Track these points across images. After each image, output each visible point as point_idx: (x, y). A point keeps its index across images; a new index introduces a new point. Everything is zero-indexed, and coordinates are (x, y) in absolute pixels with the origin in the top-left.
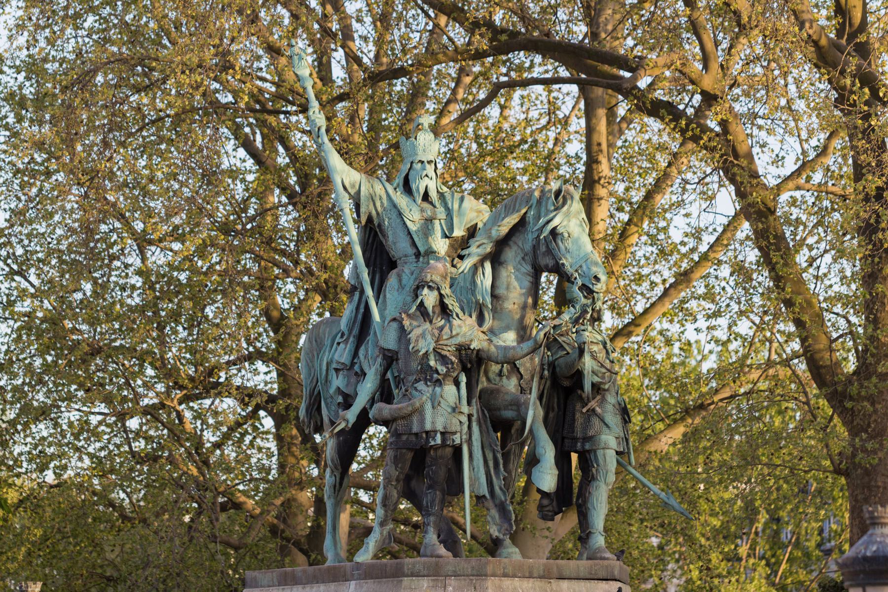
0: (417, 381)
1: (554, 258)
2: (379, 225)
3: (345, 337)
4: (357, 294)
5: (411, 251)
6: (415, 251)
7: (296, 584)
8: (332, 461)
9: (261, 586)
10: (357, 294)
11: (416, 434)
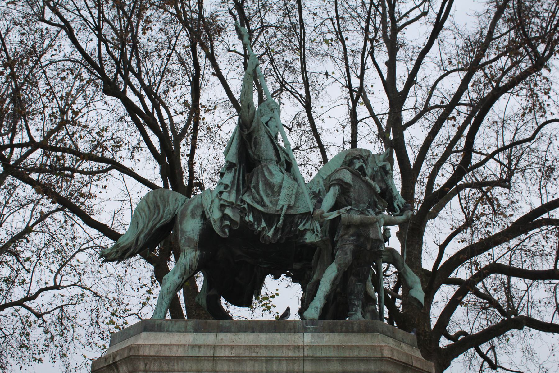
0: (368, 207)
1: (386, 184)
2: (256, 138)
3: (228, 189)
4: (233, 171)
5: (275, 158)
6: (276, 159)
8: (191, 266)
9: (167, 331)
10: (233, 171)
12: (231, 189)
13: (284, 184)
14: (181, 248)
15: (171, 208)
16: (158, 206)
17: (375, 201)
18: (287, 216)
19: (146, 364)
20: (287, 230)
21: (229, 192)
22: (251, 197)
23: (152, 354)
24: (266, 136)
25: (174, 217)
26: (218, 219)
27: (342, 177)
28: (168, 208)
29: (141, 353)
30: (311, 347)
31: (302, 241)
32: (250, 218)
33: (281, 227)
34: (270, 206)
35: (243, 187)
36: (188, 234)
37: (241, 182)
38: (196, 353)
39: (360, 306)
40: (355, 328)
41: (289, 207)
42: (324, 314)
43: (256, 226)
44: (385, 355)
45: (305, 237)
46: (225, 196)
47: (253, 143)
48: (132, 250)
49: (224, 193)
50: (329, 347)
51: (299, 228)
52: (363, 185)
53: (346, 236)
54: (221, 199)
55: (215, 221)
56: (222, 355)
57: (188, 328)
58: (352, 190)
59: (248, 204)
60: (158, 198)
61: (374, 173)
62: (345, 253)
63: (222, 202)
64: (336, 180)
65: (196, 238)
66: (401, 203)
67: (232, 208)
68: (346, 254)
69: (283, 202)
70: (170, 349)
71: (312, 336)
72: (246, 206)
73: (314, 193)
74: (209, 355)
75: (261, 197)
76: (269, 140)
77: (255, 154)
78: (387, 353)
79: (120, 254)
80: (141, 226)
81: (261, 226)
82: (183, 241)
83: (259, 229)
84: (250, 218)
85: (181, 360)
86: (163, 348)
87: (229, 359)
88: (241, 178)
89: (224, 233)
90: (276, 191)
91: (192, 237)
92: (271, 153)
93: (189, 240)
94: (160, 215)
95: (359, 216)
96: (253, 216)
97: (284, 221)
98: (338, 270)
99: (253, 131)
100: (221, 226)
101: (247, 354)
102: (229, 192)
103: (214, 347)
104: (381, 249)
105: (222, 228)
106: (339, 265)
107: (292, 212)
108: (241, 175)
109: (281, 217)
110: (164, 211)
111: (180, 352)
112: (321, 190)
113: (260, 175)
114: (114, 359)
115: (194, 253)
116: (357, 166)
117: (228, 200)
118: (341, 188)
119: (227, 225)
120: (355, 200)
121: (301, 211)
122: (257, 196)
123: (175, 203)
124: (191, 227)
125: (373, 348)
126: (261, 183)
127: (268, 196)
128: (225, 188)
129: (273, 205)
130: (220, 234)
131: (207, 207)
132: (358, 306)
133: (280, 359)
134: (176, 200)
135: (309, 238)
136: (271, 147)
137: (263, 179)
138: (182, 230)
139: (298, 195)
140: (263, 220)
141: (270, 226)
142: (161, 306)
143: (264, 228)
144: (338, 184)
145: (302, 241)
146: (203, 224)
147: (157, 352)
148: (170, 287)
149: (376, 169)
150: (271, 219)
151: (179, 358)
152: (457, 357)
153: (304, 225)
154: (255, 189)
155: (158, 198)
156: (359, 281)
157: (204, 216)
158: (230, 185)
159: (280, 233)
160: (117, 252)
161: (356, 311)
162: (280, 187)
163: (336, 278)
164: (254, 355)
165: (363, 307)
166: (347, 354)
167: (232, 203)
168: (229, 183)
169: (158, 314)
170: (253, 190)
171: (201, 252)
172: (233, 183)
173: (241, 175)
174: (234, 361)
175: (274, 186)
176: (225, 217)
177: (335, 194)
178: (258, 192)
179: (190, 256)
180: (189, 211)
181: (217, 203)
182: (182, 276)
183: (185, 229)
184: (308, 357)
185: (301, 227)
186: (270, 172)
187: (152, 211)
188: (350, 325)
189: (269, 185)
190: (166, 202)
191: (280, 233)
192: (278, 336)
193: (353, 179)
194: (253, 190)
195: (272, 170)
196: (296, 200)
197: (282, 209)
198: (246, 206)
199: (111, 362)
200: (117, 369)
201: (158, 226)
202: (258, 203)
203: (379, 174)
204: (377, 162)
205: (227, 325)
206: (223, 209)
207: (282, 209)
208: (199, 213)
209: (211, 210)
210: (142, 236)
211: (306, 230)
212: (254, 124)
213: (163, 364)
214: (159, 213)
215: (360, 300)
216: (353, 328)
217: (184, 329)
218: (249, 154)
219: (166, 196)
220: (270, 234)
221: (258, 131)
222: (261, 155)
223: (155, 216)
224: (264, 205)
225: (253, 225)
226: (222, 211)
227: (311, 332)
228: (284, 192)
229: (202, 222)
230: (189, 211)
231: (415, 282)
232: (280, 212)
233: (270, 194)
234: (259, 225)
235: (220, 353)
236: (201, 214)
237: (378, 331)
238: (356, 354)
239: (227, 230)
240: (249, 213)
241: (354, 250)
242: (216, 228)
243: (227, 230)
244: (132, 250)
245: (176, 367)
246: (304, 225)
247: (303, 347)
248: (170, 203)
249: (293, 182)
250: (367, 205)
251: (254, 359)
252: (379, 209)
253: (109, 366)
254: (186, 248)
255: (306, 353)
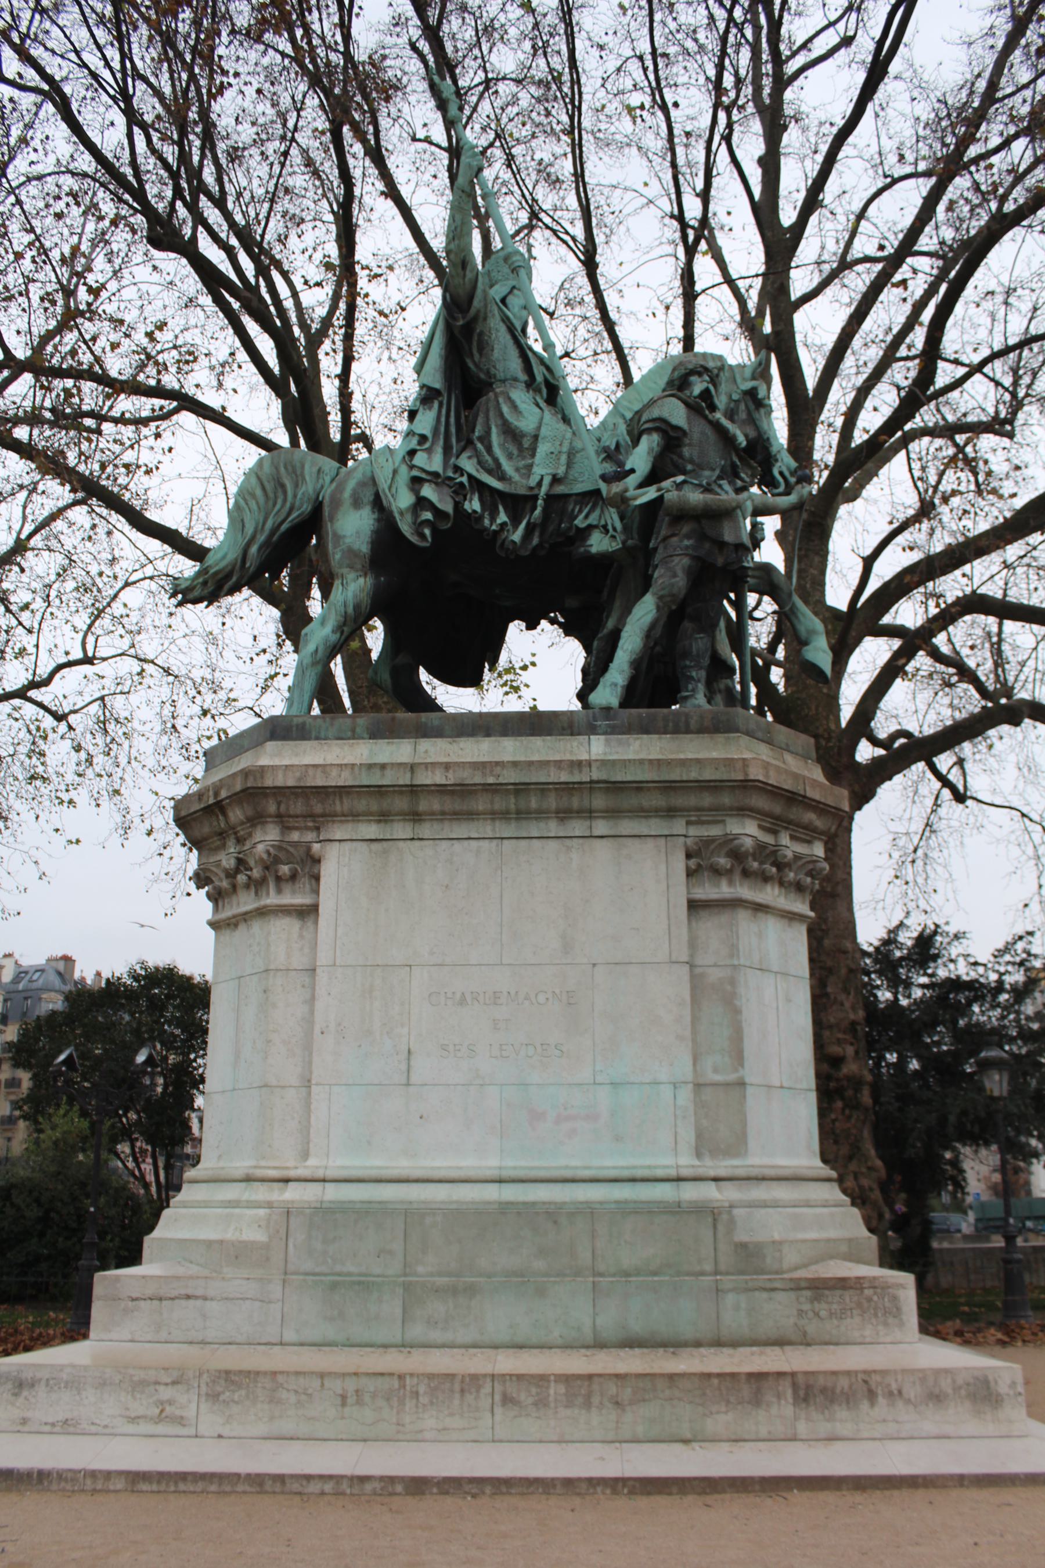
0: (720, 478)
1: (757, 428)
2: (481, 334)
3: (427, 445)
4: (436, 405)
5: (523, 377)
7: (425, 735)
8: (357, 607)
9: (317, 738)
10: (436, 405)
11: (722, 545)
12: (433, 444)
13: (544, 432)
14: (336, 569)
15: (309, 488)
16: (283, 486)
17: (734, 466)
18: (550, 498)
19: (279, 804)
20: (551, 528)
21: (429, 451)
22: (475, 460)
23: (291, 783)
24: (503, 328)
25: (318, 508)
26: (408, 509)
27: (665, 415)
28: (304, 488)
29: (269, 782)
30: (604, 763)
31: (582, 549)
32: (474, 505)
33: (538, 521)
34: (516, 477)
35: (458, 440)
36: (348, 540)
37: (453, 429)
38: (376, 779)
39: (703, 680)
40: (693, 724)
41: (556, 480)
42: (631, 697)
43: (487, 522)
44: (752, 777)
45: (589, 543)
46: (420, 459)
47: (475, 344)
48: (234, 579)
49: (419, 454)
50: (641, 762)
51: (576, 522)
52: (709, 431)
53: (675, 539)
54: (412, 467)
55: (401, 513)
56: (428, 782)
57: (358, 730)
58: (687, 441)
59: (470, 477)
60: (282, 470)
61: (732, 405)
62: (672, 574)
63: (415, 473)
64: (654, 420)
65: (365, 548)
66: (788, 469)
67: (436, 484)
68: (675, 576)
69: (542, 469)
70: (324, 772)
71: (606, 740)
72: (464, 479)
73: (606, 449)
74: (401, 782)
75: (496, 461)
76: (508, 337)
77: (481, 370)
78: (756, 773)
79: (211, 587)
80: (250, 530)
81: (499, 521)
82: (338, 556)
83: (494, 527)
84: (474, 505)
85: (348, 793)
86: (311, 772)
87: (441, 790)
88: (452, 420)
89: (422, 536)
90: (526, 446)
91: (356, 547)
92: (514, 365)
93: (351, 553)
94: (288, 505)
95: (701, 496)
96: (481, 500)
97: (545, 510)
98: (658, 608)
99: (475, 319)
100: (414, 523)
101: (478, 779)
102: (429, 451)
103: (412, 768)
104: (746, 564)
105: (419, 526)
106: (661, 598)
107: (560, 489)
108: (452, 414)
109: (540, 502)
110: (295, 496)
111: (344, 779)
112: (622, 442)
113: (492, 414)
114: (216, 794)
115: (361, 580)
116: (697, 390)
117: (428, 468)
118: (663, 438)
119: (427, 521)
120: (691, 461)
121: (579, 488)
122: (488, 458)
123: (318, 478)
124: (354, 527)
125: (729, 762)
126: (494, 430)
127: (510, 457)
128: (420, 443)
129: (522, 476)
130: (414, 539)
131: (383, 484)
132: (699, 681)
133: (543, 789)
134: (319, 471)
135: (598, 544)
136: (513, 353)
137: (500, 422)
138: (335, 534)
139: (571, 454)
140: (501, 508)
141: (516, 521)
142: (302, 690)
143: (503, 525)
144: (656, 429)
145: (582, 549)
146: (378, 520)
147: (300, 779)
148: (316, 651)
149: (735, 397)
150: (518, 504)
151: (342, 791)
152: (890, 779)
153: (586, 517)
154: (482, 443)
155: (282, 470)
156: (701, 630)
157: (378, 504)
158: (429, 434)
159: (537, 534)
160: (205, 583)
161: (693, 690)
162: (536, 437)
163: (653, 626)
164: (491, 780)
165: (709, 684)
166: (676, 775)
167: (436, 474)
168: (427, 432)
169: (295, 704)
170: (479, 446)
171: (377, 577)
172: (436, 431)
173: (452, 414)
174: (452, 793)
175: (523, 435)
176: (421, 503)
177: (651, 450)
178: (489, 449)
179: (354, 587)
180: (347, 494)
181: (404, 474)
182: (339, 628)
183: (340, 532)
184: (598, 782)
185: (580, 522)
186: (514, 407)
187: (271, 495)
188: (683, 719)
189: (511, 433)
190: (298, 479)
191: (537, 534)
192: (538, 742)
193: (688, 418)
194: (479, 446)
195: (518, 402)
196: (569, 465)
197: (540, 484)
198: (464, 479)
199: (211, 801)
200: (225, 815)
201: (285, 527)
202: (490, 472)
203: (742, 407)
204: (739, 380)
205: (436, 723)
206: (417, 486)
207: (540, 484)
208: (368, 496)
209: (394, 490)
210: (254, 549)
211: (590, 528)
212: (477, 303)
213: (313, 802)
214: (285, 500)
215: (701, 668)
216: (687, 724)
217: (349, 734)
218: (469, 369)
219: (298, 465)
220: (517, 536)
221: (485, 319)
222: (493, 371)
223: (278, 506)
224: (502, 477)
225: (480, 518)
226: (416, 492)
227: (605, 733)
228: (543, 449)
229: (376, 516)
230: (347, 494)
231: (812, 632)
232: (536, 492)
233: (515, 452)
234: (493, 519)
235: (425, 778)
236: (372, 498)
237: (737, 731)
238: (694, 775)
239: (427, 532)
240: (473, 493)
241: (690, 567)
242: (406, 528)
243: (427, 532)
244: (234, 579)
245: (338, 808)
246: (586, 517)
247: (589, 763)
248: (307, 478)
249: (562, 426)
250: (717, 472)
251: (493, 789)
252: (742, 480)
253: (208, 810)
254: (345, 571)
255: (596, 775)
